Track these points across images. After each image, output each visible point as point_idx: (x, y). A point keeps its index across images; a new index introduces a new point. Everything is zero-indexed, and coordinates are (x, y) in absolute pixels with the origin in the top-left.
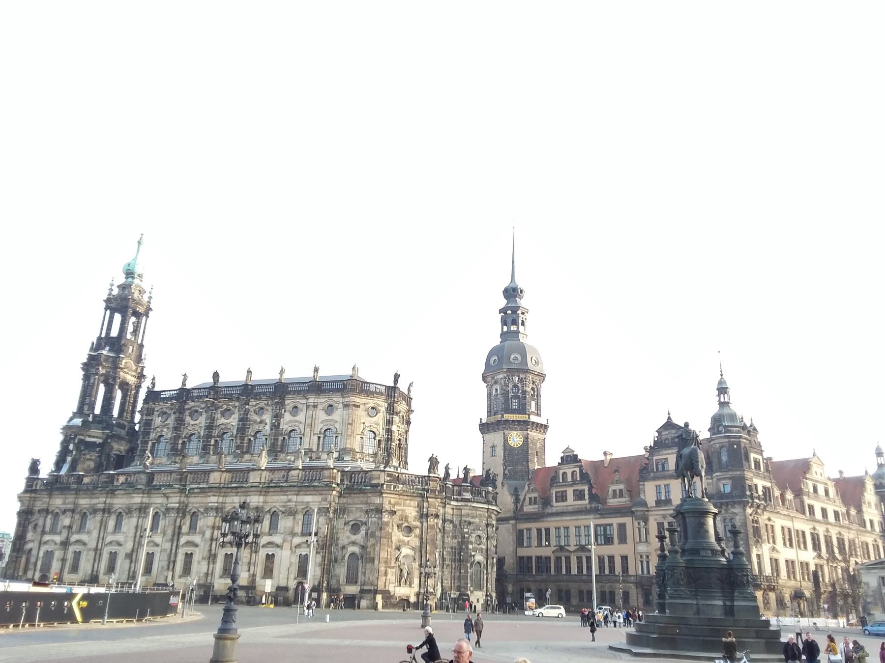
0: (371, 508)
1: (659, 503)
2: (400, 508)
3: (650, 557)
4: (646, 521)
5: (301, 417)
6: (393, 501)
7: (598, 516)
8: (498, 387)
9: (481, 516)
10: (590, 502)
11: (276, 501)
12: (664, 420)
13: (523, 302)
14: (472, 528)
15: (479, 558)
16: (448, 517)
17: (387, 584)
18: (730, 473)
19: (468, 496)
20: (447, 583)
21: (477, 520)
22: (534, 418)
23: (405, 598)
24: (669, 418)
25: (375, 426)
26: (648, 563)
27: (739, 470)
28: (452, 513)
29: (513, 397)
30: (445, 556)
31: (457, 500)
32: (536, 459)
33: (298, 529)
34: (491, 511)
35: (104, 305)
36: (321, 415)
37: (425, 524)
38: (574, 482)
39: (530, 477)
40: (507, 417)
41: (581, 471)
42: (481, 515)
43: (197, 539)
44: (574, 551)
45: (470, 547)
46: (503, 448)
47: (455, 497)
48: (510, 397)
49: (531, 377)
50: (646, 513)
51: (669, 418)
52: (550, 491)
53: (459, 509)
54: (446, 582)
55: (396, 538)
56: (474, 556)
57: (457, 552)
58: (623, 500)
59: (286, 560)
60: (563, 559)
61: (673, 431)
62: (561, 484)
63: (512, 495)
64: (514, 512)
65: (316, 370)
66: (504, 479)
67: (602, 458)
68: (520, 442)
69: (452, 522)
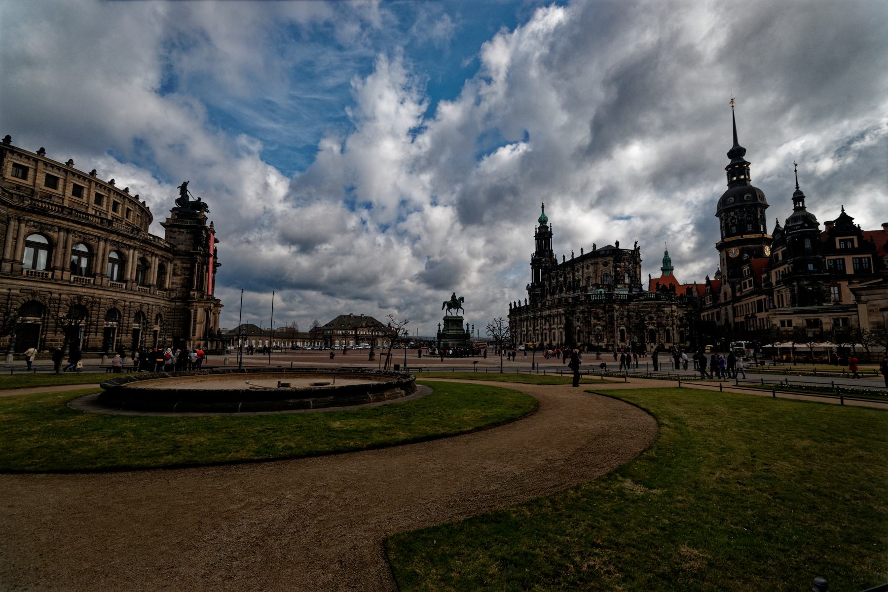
5: (580, 273)
8: (723, 221)
10: (754, 288)
11: (554, 311)
15: (651, 327)
16: (632, 310)
21: (649, 309)
22: (745, 237)
29: (731, 226)
31: (636, 301)
33: (559, 322)
35: (534, 238)
36: (586, 270)
40: (727, 240)
43: (538, 328)
59: (557, 333)
65: (582, 250)
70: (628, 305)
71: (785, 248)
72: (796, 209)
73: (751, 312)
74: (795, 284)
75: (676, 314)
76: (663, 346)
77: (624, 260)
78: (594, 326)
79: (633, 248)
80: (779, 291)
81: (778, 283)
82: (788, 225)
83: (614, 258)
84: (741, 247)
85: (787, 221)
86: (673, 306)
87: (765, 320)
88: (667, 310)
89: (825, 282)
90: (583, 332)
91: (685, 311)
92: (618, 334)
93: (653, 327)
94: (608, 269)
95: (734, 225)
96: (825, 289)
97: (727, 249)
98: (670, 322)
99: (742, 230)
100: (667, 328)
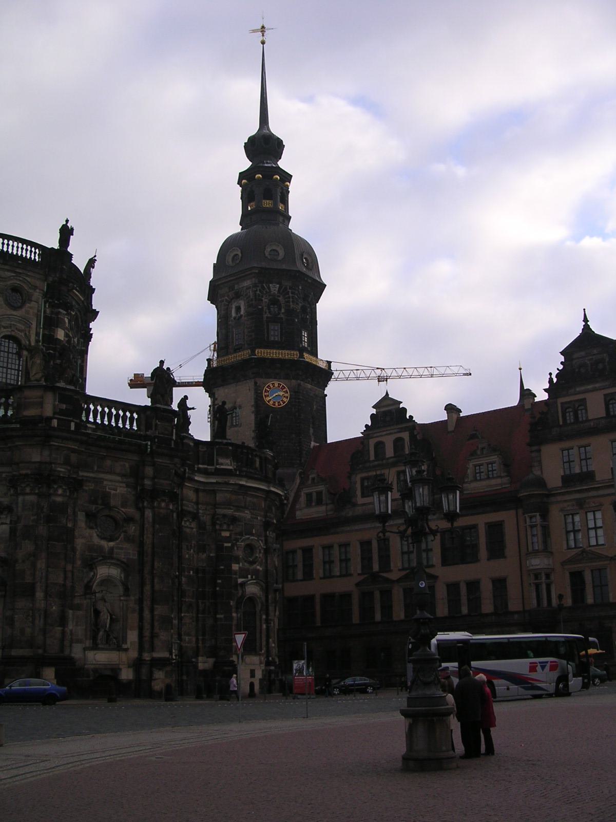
0: (24, 472)
1: (568, 480)
2: (91, 475)
3: (552, 577)
6: (74, 458)
12: (577, 331)
13: (283, 164)
15: (252, 589)
16: (190, 507)
17: (67, 643)
20: (189, 641)
21: (247, 514)
22: (307, 357)
23: (108, 673)
24: (586, 328)
25: (23, 327)
26: (548, 586)
28: (194, 500)
30: (185, 587)
31: (206, 473)
32: (311, 431)
37: (148, 513)
38: (400, 458)
39: (303, 461)
40: (261, 353)
41: (413, 438)
44: (398, 581)
45: (235, 567)
46: (253, 409)
47: (201, 466)
48: (265, 319)
49: (300, 288)
51: (586, 328)
52: (349, 477)
53: (212, 491)
54: (187, 638)
55: (83, 541)
56: (243, 585)
58: (499, 481)
60: (377, 595)
61: (595, 351)
62: (371, 464)
67: (444, 416)
68: (285, 399)
69: (195, 517)
73: (396, 562)
78: (90, 565)
84: (294, 382)
87: (487, 589)
90: (30, 591)
97: (260, 381)
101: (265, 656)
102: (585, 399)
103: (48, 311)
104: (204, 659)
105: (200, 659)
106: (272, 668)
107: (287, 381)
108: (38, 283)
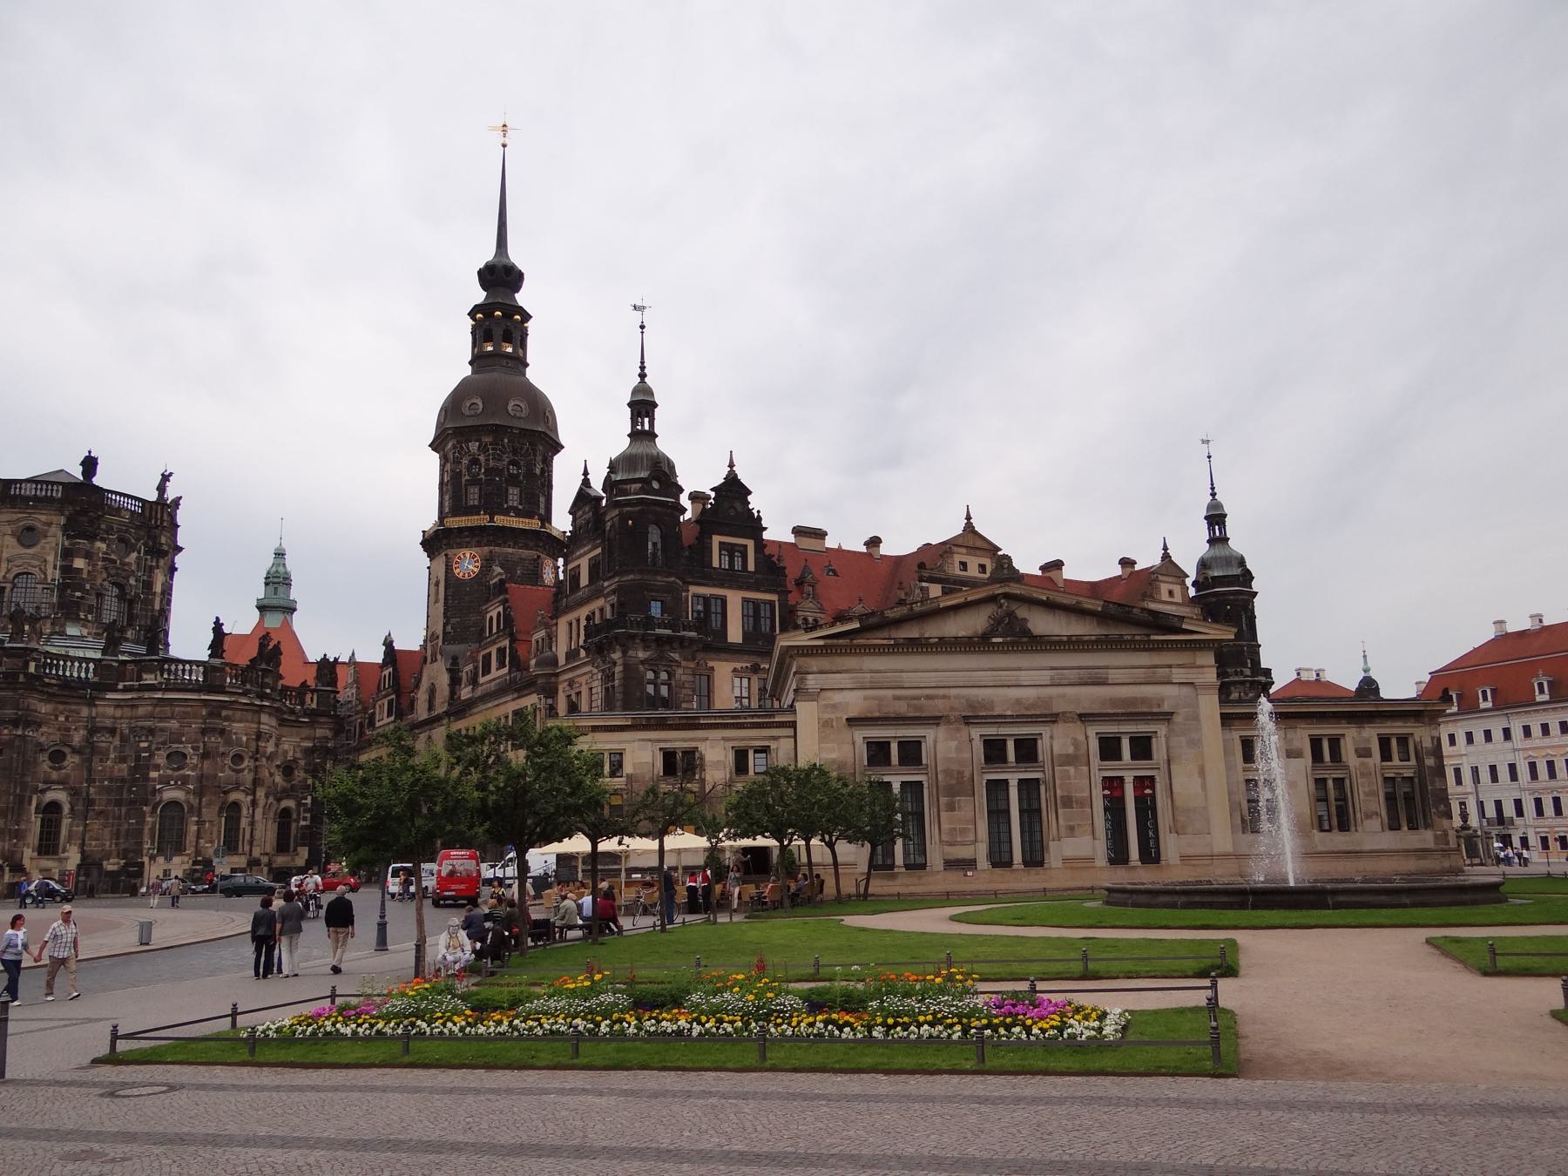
4: (551, 692)
7: (516, 695)
8: (448, 467)
9: (185, 715)
10: (510, 672)
14: (161, 740)
16: (108, 723)
18: (616, 580)
19: (149, 679)
22: (500, 520)
25: (37, 563)
27: (632, 572)
29: (469, 483)
31: (126, 690)
34: (214, 704)
40: (454, 522)
42: (184, 712)
48: (463, 483)
49: (506, 441)
50: (553, 679)
54: (94, 843)
57: (127, 785)
63: (449, 670)
64: (449, 704)
66: (443, 643)
68: (476, 570)
69: (112, 731)
70: (91, 703)
71: (599, 550)
72: (635, 435)
74: (617, 656)
75: (270, 748)
76: (208, 863)
77: (109, 530)
79: (152, 496)
80: (571, 683)
81: (572, 655)
82: (613, 476)
83: (69, 519)
85: (613, 467)
86: (264, 718)
88: (240, 729)
89: (686, 659)
91: (307, 738)
92: (35, 824)
93: (178, 795)
94: (34, 556)
95: (474, 481)
96: (684, 678)
97: (450, 552)
98: (248, 777)
99: (493, 504)
100: (233, 796)
101: (193, 855)
102: (579, 566)
103: (66, 543)
104: (116, 860)
105: (111, 861)
106: (198, 867)
107: (478, 549)
108: (55, 519)
